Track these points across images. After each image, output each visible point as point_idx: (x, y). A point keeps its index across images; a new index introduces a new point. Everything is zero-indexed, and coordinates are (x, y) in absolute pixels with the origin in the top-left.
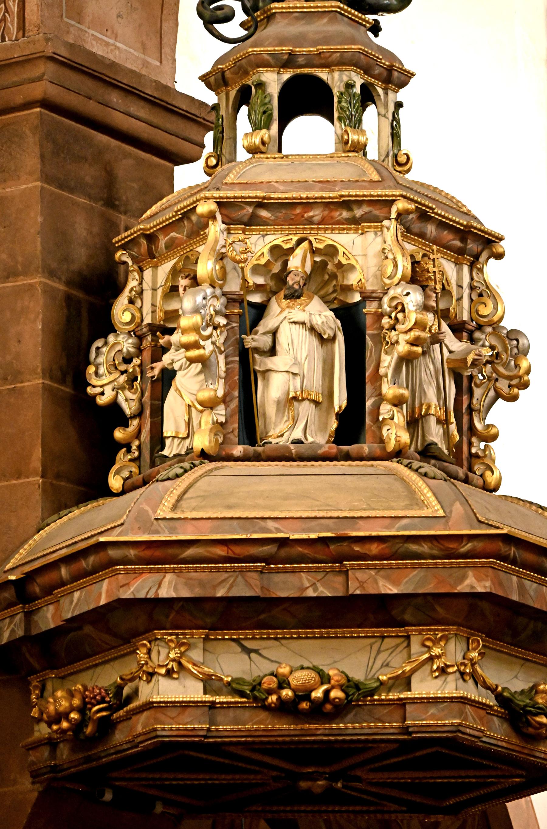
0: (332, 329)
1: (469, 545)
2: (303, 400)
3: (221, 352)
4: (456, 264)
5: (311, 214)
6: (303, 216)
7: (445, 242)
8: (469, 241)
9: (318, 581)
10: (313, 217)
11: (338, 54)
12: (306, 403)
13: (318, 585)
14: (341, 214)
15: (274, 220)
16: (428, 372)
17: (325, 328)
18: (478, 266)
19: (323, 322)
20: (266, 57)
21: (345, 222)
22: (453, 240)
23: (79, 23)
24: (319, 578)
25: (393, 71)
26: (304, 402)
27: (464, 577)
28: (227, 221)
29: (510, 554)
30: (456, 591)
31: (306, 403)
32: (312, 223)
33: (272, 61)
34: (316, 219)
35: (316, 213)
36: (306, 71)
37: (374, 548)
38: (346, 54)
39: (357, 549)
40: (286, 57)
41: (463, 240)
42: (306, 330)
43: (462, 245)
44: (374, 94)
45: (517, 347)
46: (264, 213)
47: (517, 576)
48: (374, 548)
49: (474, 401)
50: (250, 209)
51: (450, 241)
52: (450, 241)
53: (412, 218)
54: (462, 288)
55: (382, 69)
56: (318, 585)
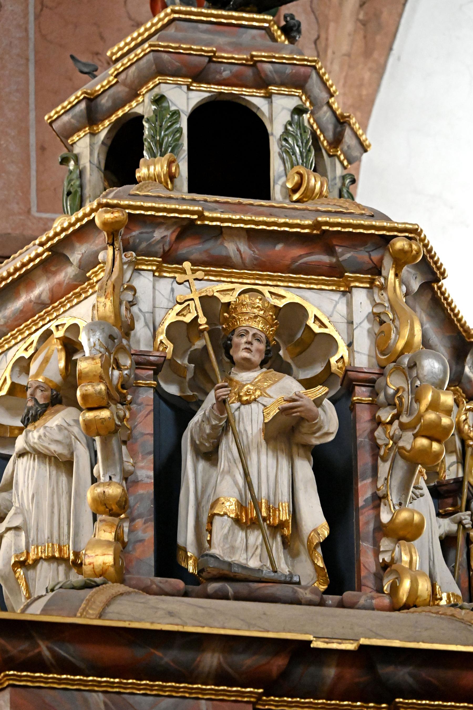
0: (57, 442)
2: (36, 561)
4: (344, 293)
8: (339, 250)
10: (40, 295)
12: (43, 567)
14: (66, 274)
16: (230, 456)
17: (46, 445)
18: (377, 283)
19: (40, 437)
21: (75, 283)
22: (308, 254)
25: (259, 64)
26: (39, 565)
31: (43, 567)
36: (120, 113)
40: (83, 105)
41: (331, 251)
42: (34, 459)
43: (334, 260)
44: (255, 110)
45: (417, 377)
49: (380, 484)
51: (301, 257)
52: (301, 257)
54: (352, 323)
55: (235, 68)
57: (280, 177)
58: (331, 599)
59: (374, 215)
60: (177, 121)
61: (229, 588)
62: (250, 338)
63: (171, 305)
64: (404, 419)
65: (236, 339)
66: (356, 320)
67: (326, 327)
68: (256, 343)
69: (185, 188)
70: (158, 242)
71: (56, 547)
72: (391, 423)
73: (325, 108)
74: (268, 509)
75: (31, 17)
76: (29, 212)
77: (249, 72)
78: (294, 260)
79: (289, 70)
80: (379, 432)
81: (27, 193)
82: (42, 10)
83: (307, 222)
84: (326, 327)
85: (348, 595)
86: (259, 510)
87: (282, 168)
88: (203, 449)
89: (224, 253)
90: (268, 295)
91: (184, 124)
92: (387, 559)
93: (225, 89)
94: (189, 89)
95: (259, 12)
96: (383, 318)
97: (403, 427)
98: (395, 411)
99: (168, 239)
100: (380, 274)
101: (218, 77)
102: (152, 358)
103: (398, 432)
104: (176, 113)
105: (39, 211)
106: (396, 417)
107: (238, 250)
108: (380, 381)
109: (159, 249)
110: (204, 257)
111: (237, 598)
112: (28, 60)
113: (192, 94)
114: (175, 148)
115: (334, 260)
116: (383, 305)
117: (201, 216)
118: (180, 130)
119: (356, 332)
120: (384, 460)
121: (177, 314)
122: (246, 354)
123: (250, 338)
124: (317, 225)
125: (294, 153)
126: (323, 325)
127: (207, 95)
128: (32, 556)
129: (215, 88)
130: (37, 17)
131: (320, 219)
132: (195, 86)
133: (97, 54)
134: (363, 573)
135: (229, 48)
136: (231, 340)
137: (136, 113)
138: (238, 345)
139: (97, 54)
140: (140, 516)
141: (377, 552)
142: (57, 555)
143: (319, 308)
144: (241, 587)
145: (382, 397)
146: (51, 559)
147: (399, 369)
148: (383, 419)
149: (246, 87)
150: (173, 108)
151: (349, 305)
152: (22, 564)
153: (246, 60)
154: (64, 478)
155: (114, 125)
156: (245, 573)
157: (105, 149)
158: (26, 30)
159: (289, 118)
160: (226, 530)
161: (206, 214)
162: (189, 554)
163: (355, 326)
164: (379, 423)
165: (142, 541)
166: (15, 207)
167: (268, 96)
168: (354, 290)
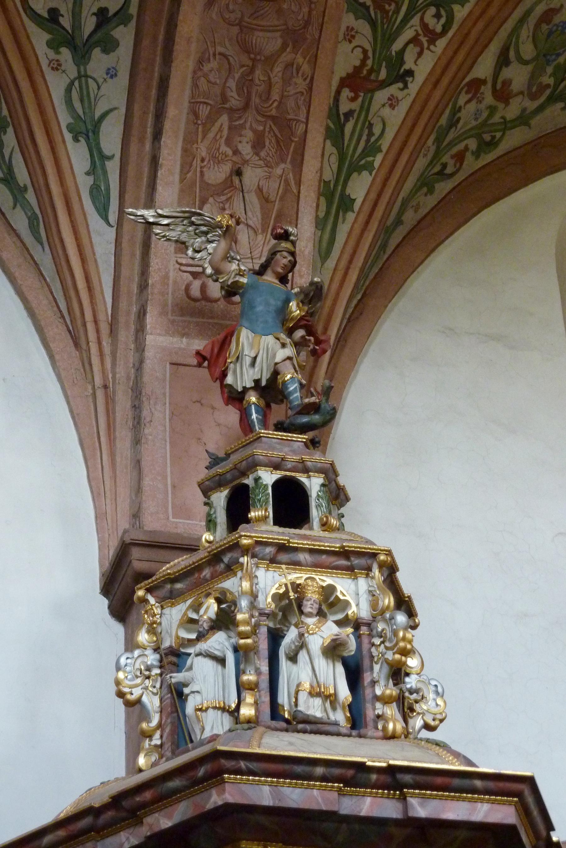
1: (202, 769)
3: (155, 694)
5: (204, 574)
6: (200, 578)
7: (328, 564)
8: (352, 559)
9: (130, 834)
10: (205, 575)
11: (245, 462)
12: (211, 711)
13: (131, 837)
15: (185, 589)
20: (207, 483)
23: (189, 519)
24: (131, 832)
25: (305, 462)
26: (209, 710)
27: (210, 796)
28: (158, 601)
29: (241, 766)
30: (206, 810)
31: (211, 711)
32: (207, 581)
33: (212, 485)
34: (208, 576)
35: (207, 573)
37: (148, 795)
38: (249, 460)
39: (138, 799)
43: (349, 564)
46: (179, 586)
47: (269, 785)
48: (148, 795)
49: (375, 675)
50: (168, 586)
51: (334, 562)
52: (334, 562)
53: (270, 552)
54: (358, 594)
55: (294, 464)
56: (131, 837)
57: (316, 518)
58: (354, 733)
59: (368, 542)
60: (267, 489)
61: (308, 727)
62: (312, 603)
63: (273, 584)
64: (388, 644)
65: (305, 602)
66: (360, 593)
67: (345, 596)
68: (315, 605)
69: (272, 523)
70: (268, 554)
71: (217, 702)
72: (380, 645)
73: (333, 482)
74: (324, 689)
75: (168, 420)
76: (168, 518)
77: (300, 466)
78: (331, 563)
79: (319, 465)
80: (373, 649)
81: (167, 508)
82: (172, 417)
83: (338, 545)
84: (345, 596)
85: (363, 731)
86: (320, 688)
87: (316, 514)
88: (290, 656)
89: (298, 559)
90: (318, 580)
91: (270, 491)
92: (380, 713)
93: (288, 473)
94: (272, 473)
95: (301, 434)
96: (375, 593)
97: (387, 648)
98: (382, 639)
99: (272, 553)
100: (371, 571)
101: (285, 467)
102: (266, 612)
103: (384, 650)
104: (266, 486)
105: (173, 518)
106: (383, 642)
107: (305, 558)
108: (374, 624)
109: (268, 557)
110: (289, 561)
111: (311, 732)
112: (166, 441)
113: (273, 475)
114: (267, 502)
115: (349, 564)
116: (373, 586)
117: (289, 542)
118: (268, 494)
119: (360, 599)
120: (376, 663)
121: (276, 589)
122: (310, 610)
123: (312, 603)
124: (343, 547)
125: (322, 506)
126: (344, 595)
127: (280, 476)
128: (205, 705)
129: (284, 473)
130: (170, 420)
131: (344, 544)
132: (274, 472)
133: (199, 439)
134: (368, 719)
135: (291, 453)
136: (302, 602)
137: (244, 483)
138: (306, 605)
139: (199, 439)
140: (263, 690)
141: (374, 709)
142: (218, 706)
143: (342, 587)
144: (314, 727)
145: (374, 632)
146: (215, 708)
147: (385, 620)
148: (376, 643)
149: (298, 472)
150: (264, 483)
151: (357, 585)
152: (200, 710)
153: (299, 460)
154: (220, 667)
155: (233, 487)
156: (313, 719)
157: (227, 499)
158: (165, 426)
159: (319, 489)
160: (305, 698)
161: (291, 540)
162: (286, 709)
163: (360, 596)
164: (373, 645)
165: (263, 702)
166: (161, 516)
167: (309, 477)
168: (359, 578)
